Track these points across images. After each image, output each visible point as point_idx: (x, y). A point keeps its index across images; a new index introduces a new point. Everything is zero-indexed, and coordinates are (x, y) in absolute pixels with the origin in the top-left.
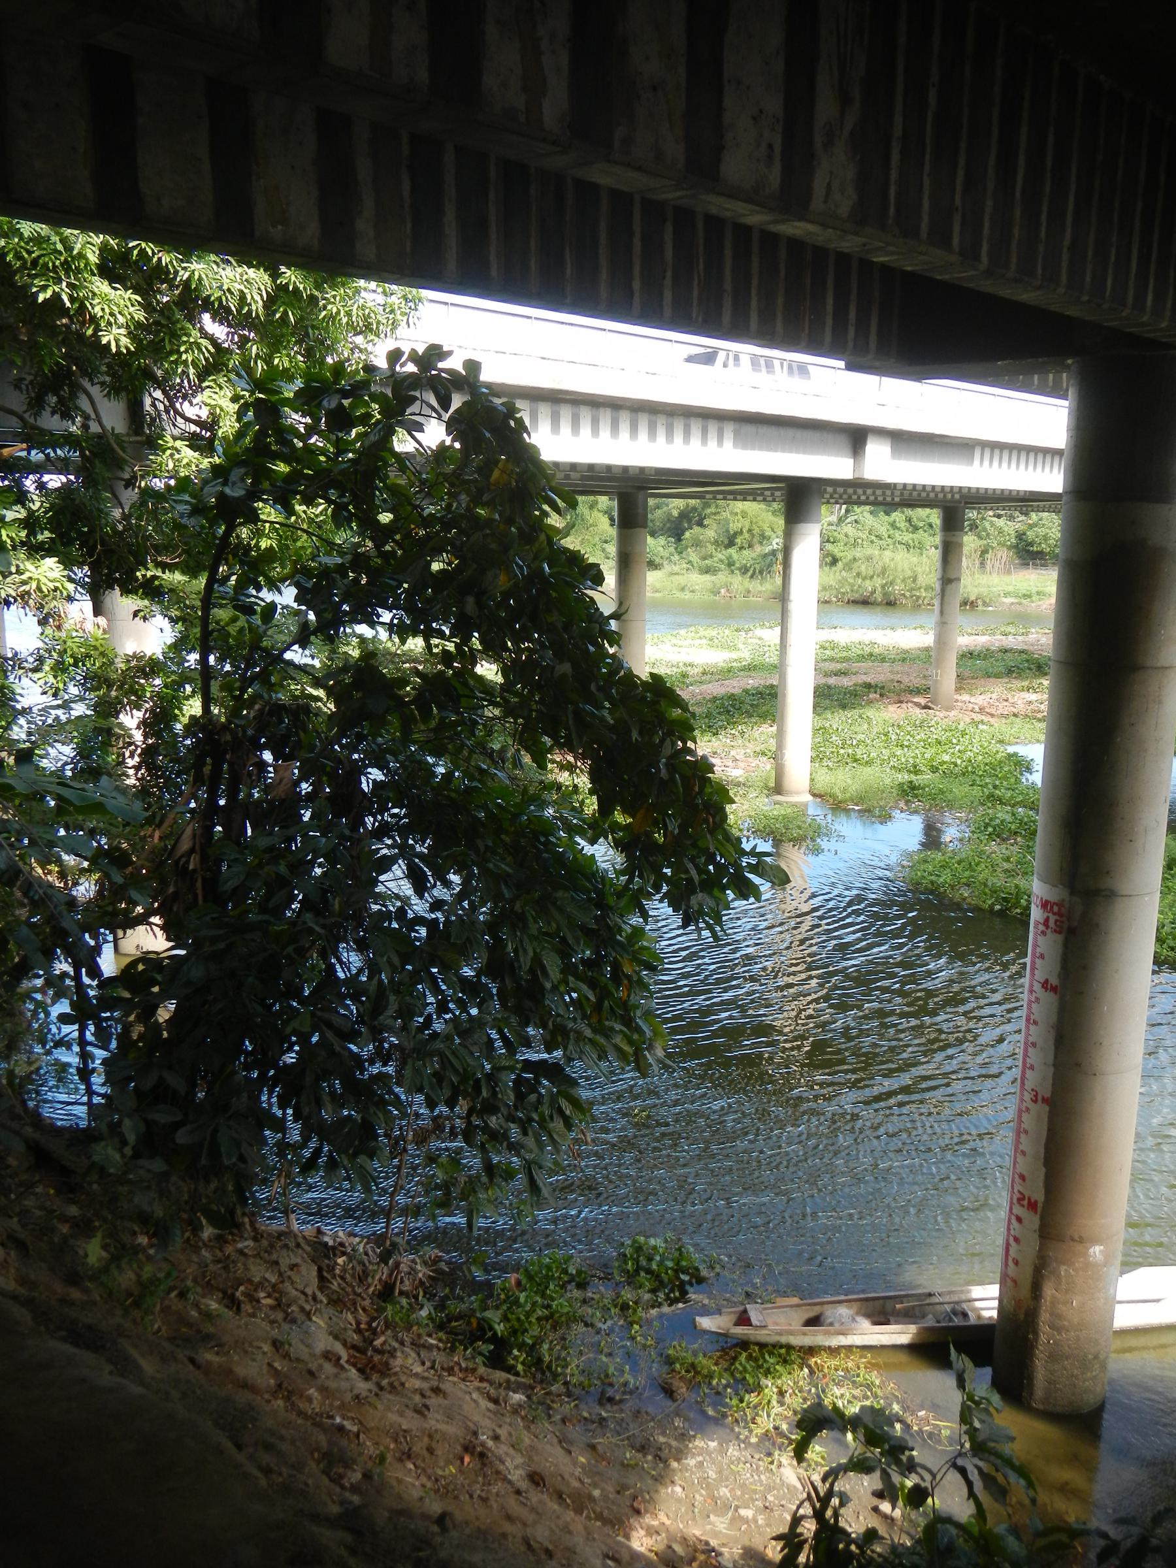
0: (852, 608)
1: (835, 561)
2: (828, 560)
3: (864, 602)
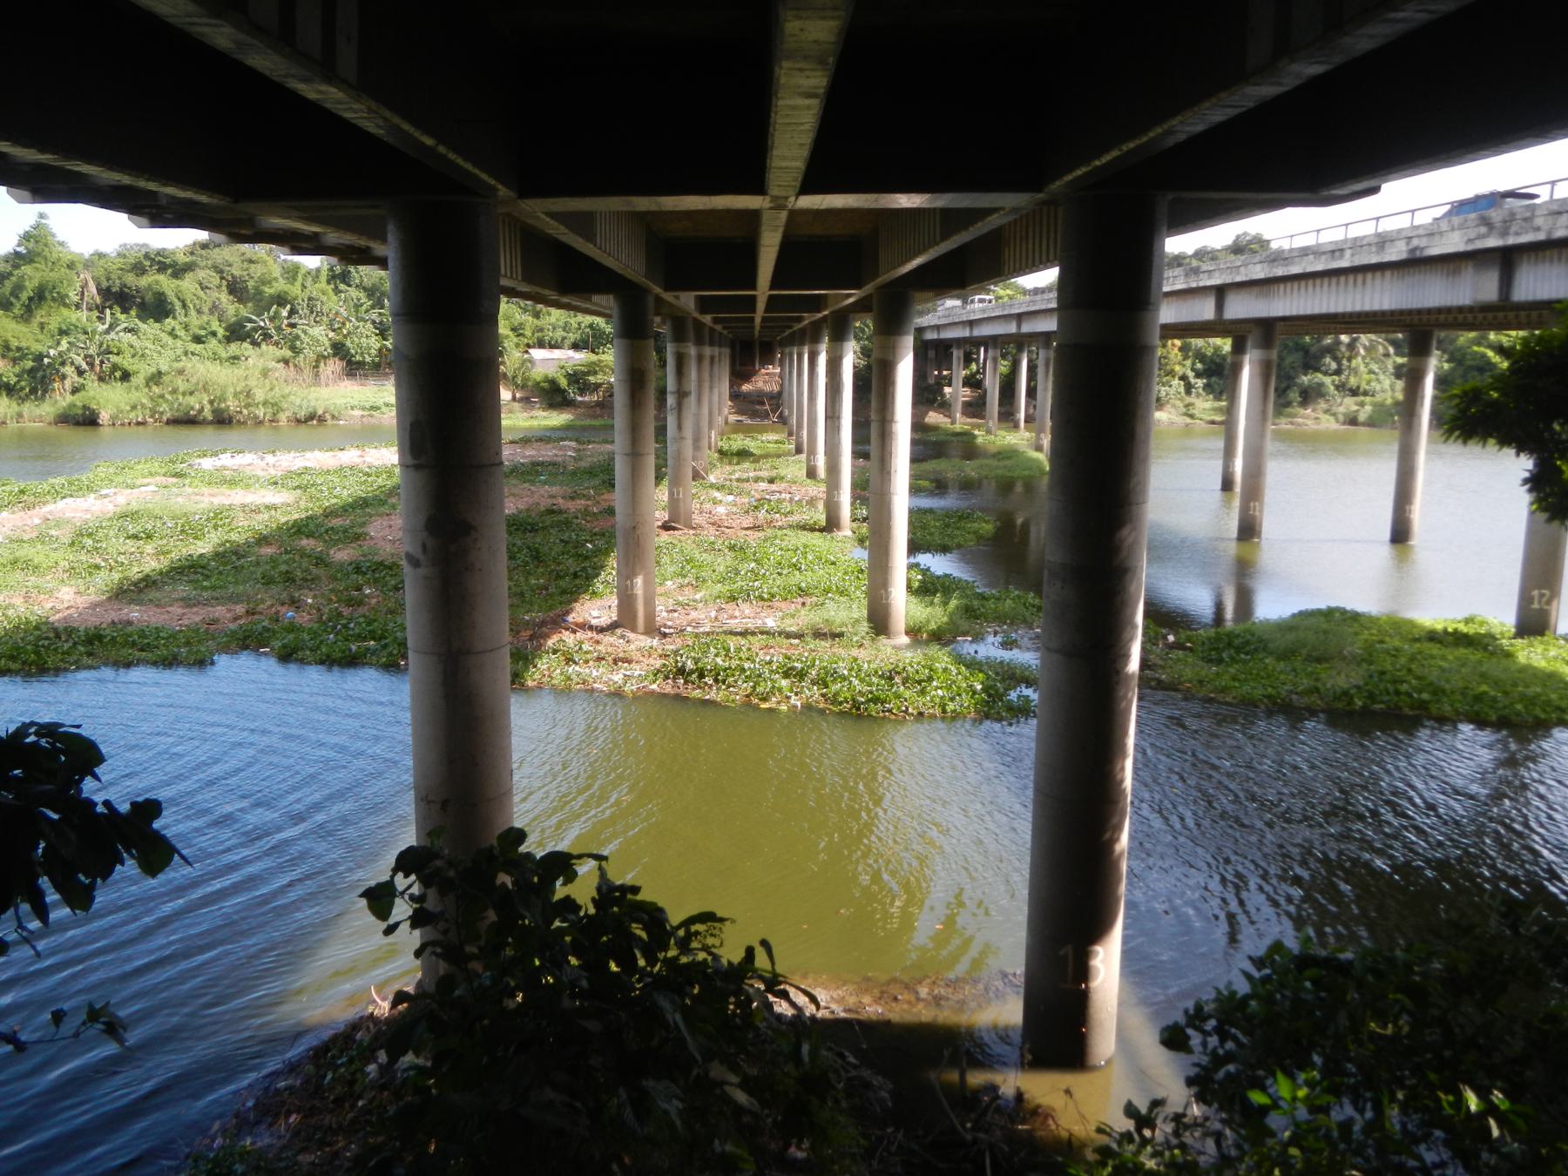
0: (170, 430)
1: (126, 376)
2: (118, 374)
3: (187, 421)
